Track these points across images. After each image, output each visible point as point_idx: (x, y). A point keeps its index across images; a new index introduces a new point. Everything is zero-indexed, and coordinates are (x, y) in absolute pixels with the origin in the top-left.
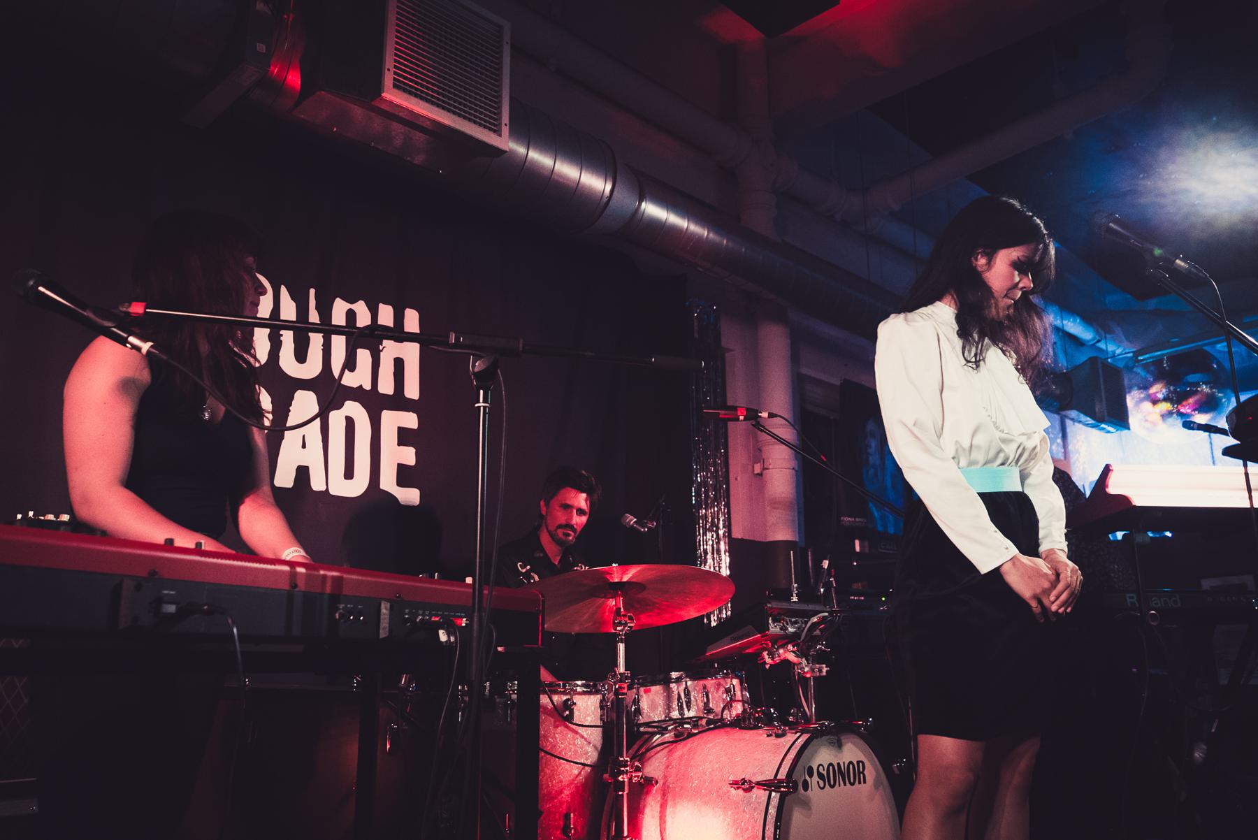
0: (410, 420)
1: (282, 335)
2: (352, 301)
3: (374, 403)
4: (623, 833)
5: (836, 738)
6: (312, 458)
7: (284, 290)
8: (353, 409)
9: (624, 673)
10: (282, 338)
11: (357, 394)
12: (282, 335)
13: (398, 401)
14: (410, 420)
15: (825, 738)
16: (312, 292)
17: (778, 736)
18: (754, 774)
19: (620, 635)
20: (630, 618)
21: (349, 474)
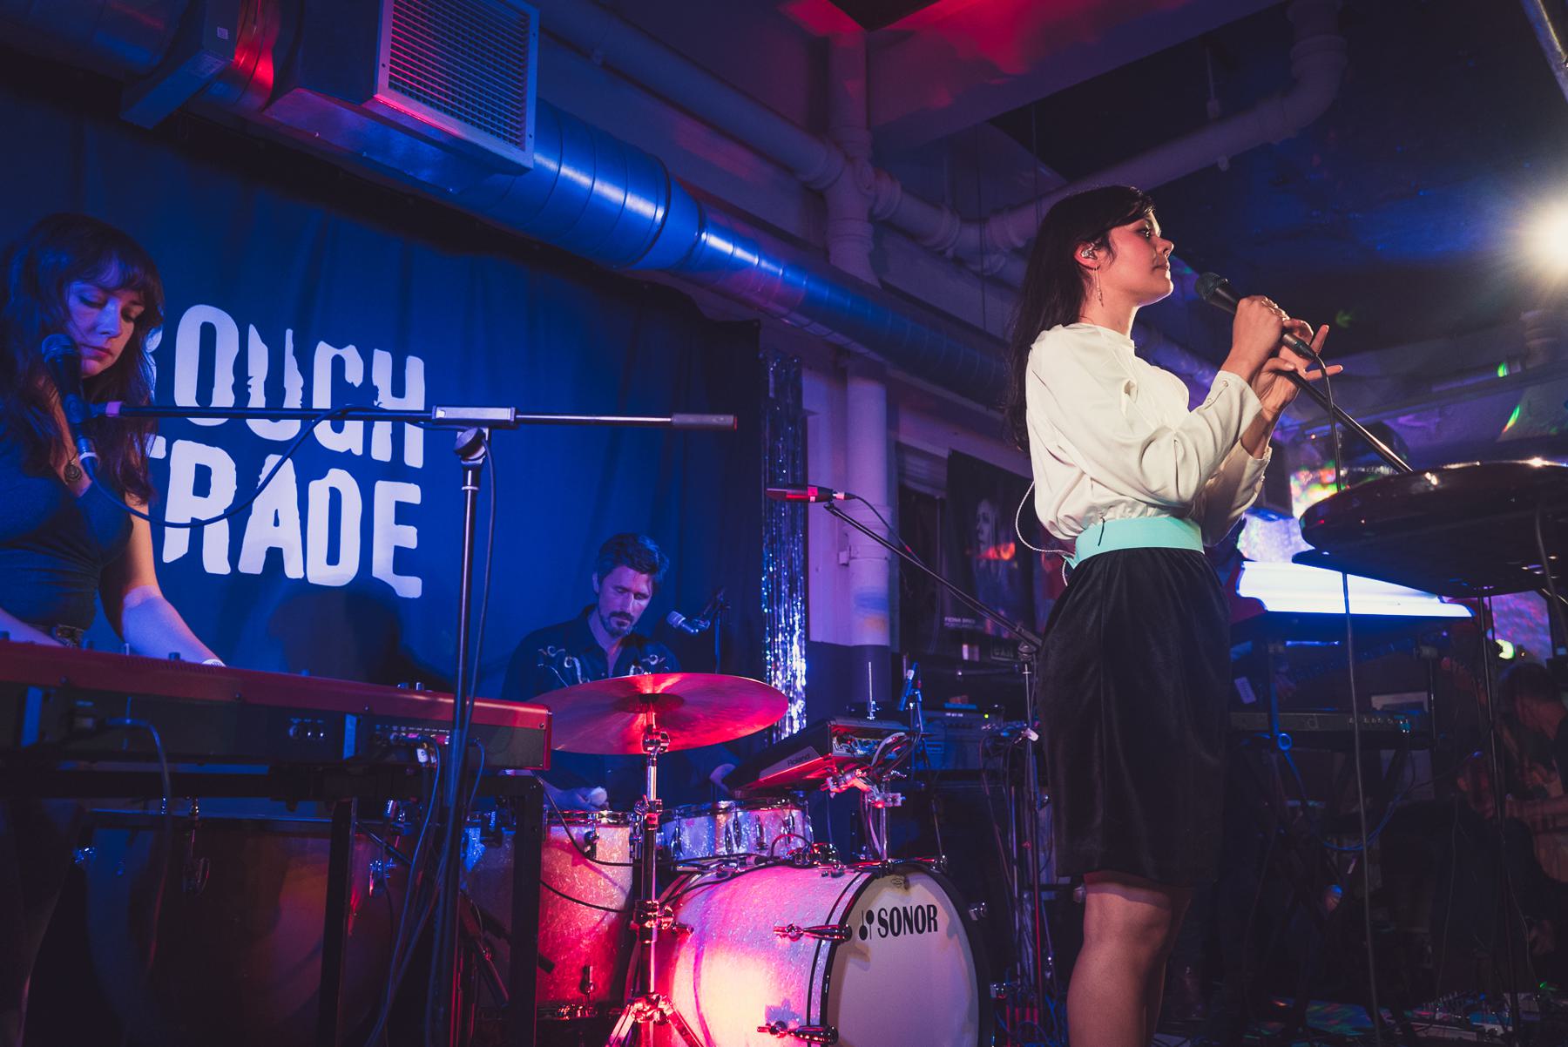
0: (412, 494)
1: (250, 386)
2: (340, 347)
3: (366, 471)
4: (649, 988)
5: (903, 878)
6: (288, 537)
7: (253, 332)
8: (339, 478)
9: (655, 802)
10: (250, 390)
11: (344, 460)
12: (250, 386)
13: (396, 470)
14: (412, 494)
15: (889, 878)
16: (289, 333)
17: (835, 876)
18: (804, 919)
19: (650, 756)
20: (664, 737)
21: (333, 558)
